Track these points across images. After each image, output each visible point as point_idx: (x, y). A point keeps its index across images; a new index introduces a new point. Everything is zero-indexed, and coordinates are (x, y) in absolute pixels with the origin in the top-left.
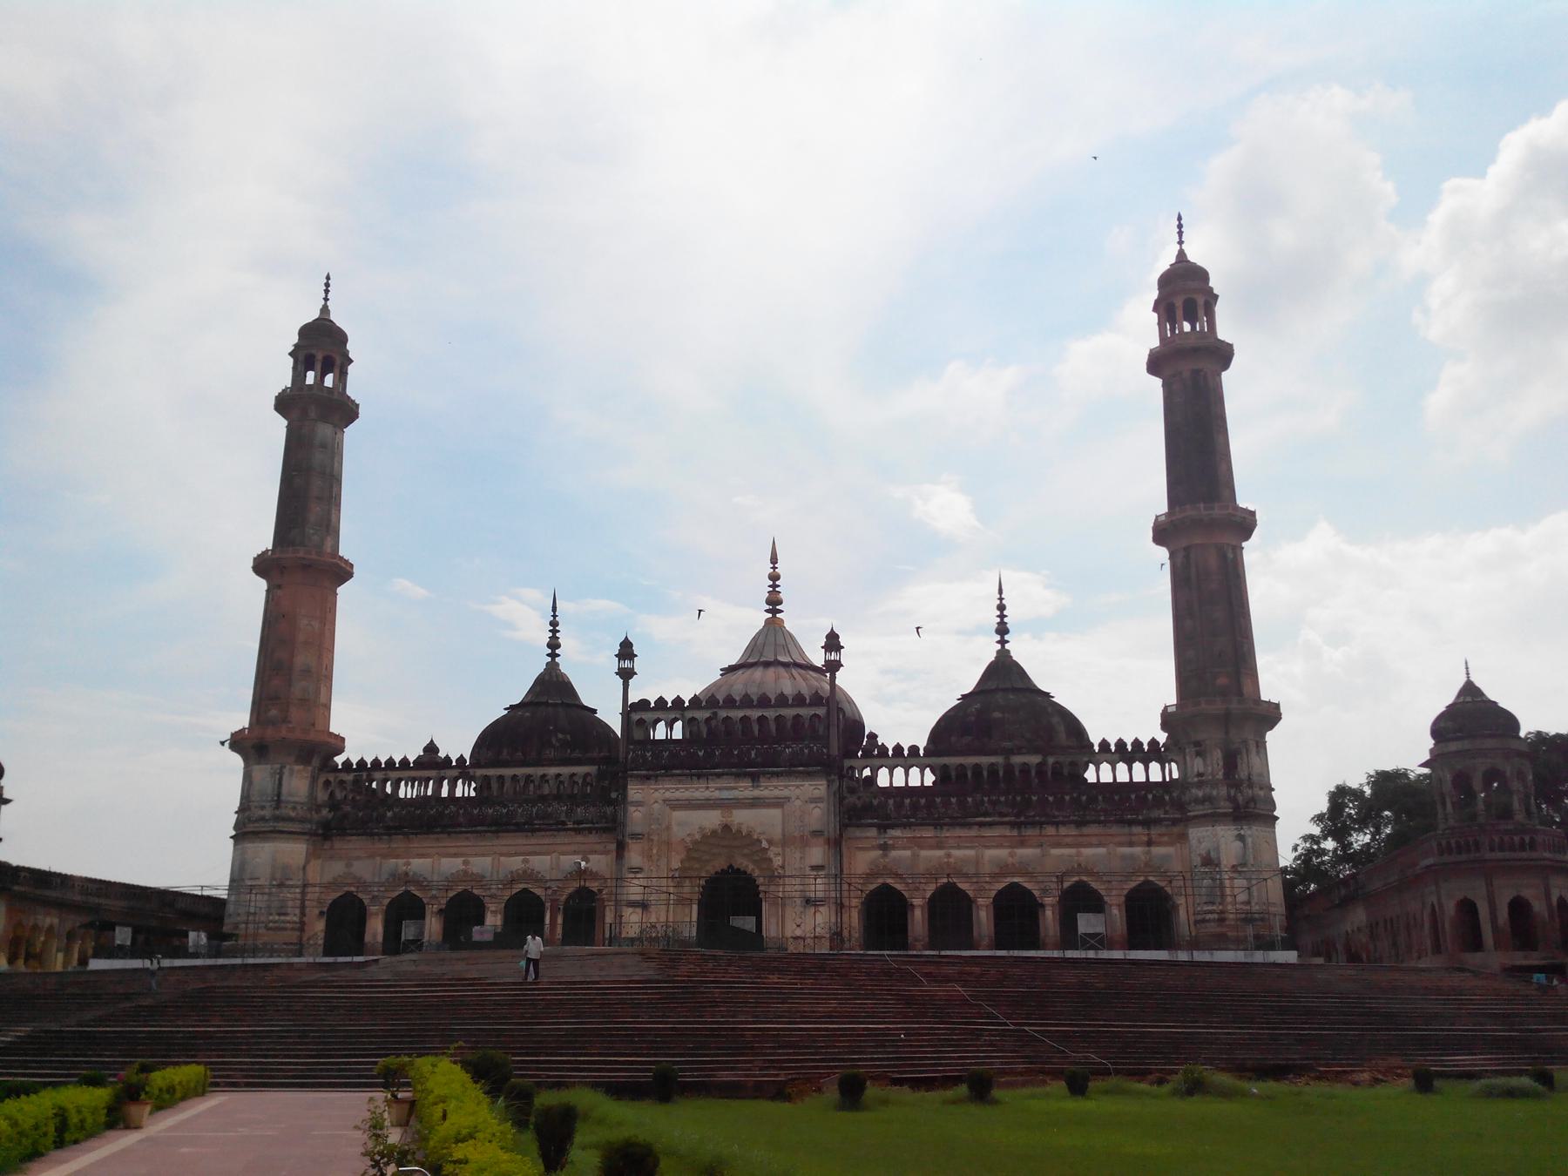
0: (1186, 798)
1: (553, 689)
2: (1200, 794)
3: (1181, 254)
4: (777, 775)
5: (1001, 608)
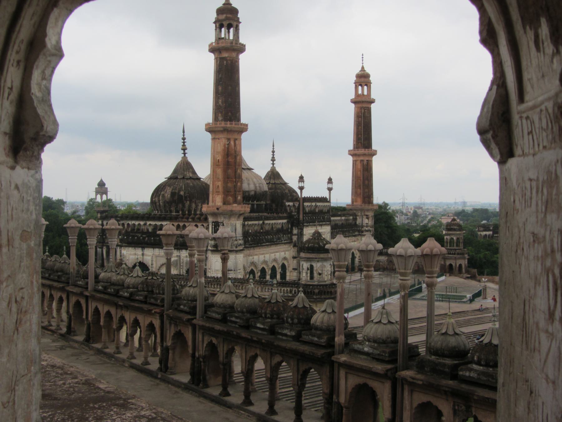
0: (363, 229)
1: (184, 169)
2: (367, 229)
3: (363, 68)
4: (325, 225)
5: (273, 152)
